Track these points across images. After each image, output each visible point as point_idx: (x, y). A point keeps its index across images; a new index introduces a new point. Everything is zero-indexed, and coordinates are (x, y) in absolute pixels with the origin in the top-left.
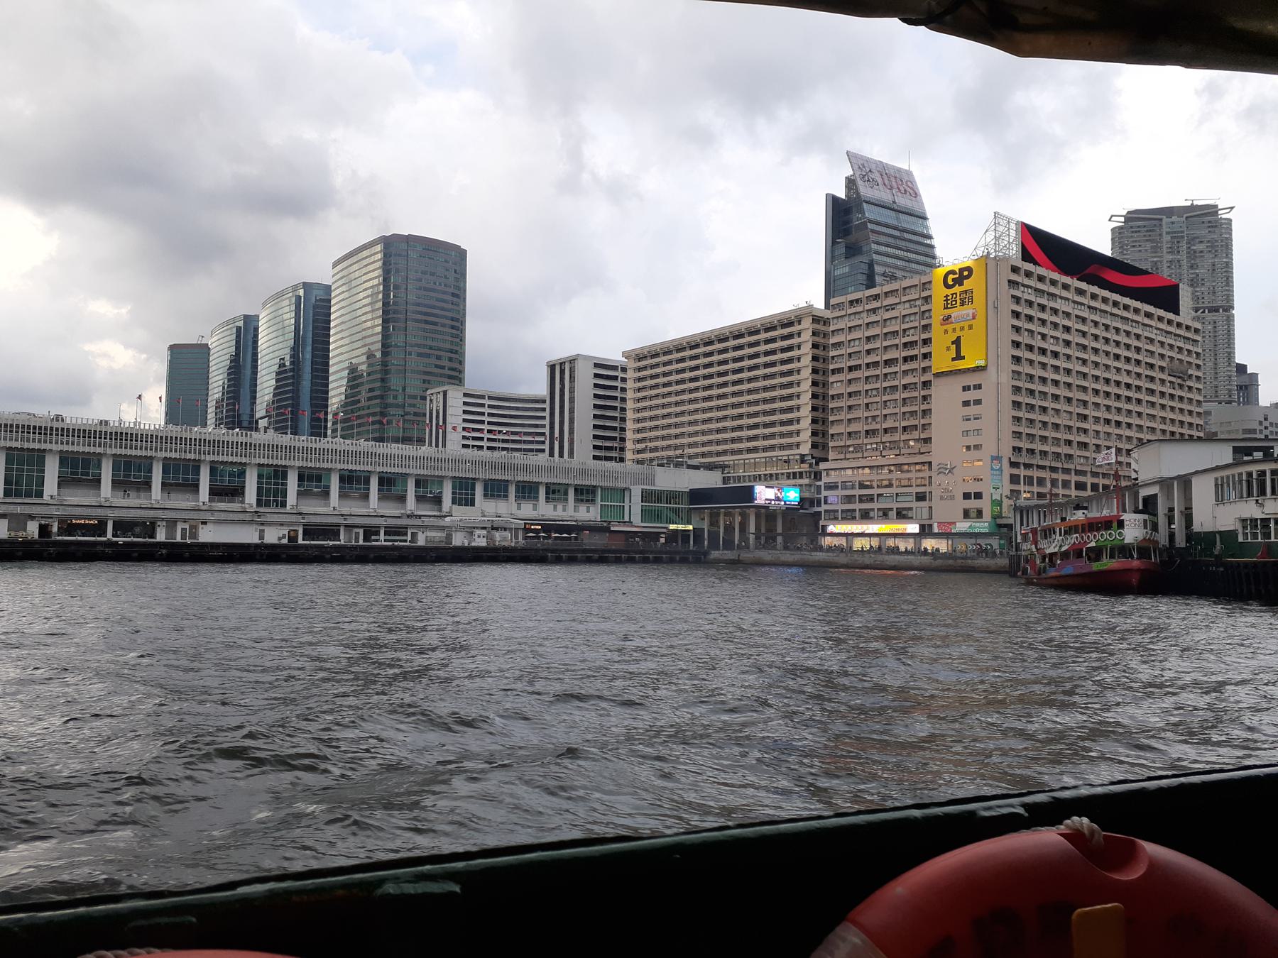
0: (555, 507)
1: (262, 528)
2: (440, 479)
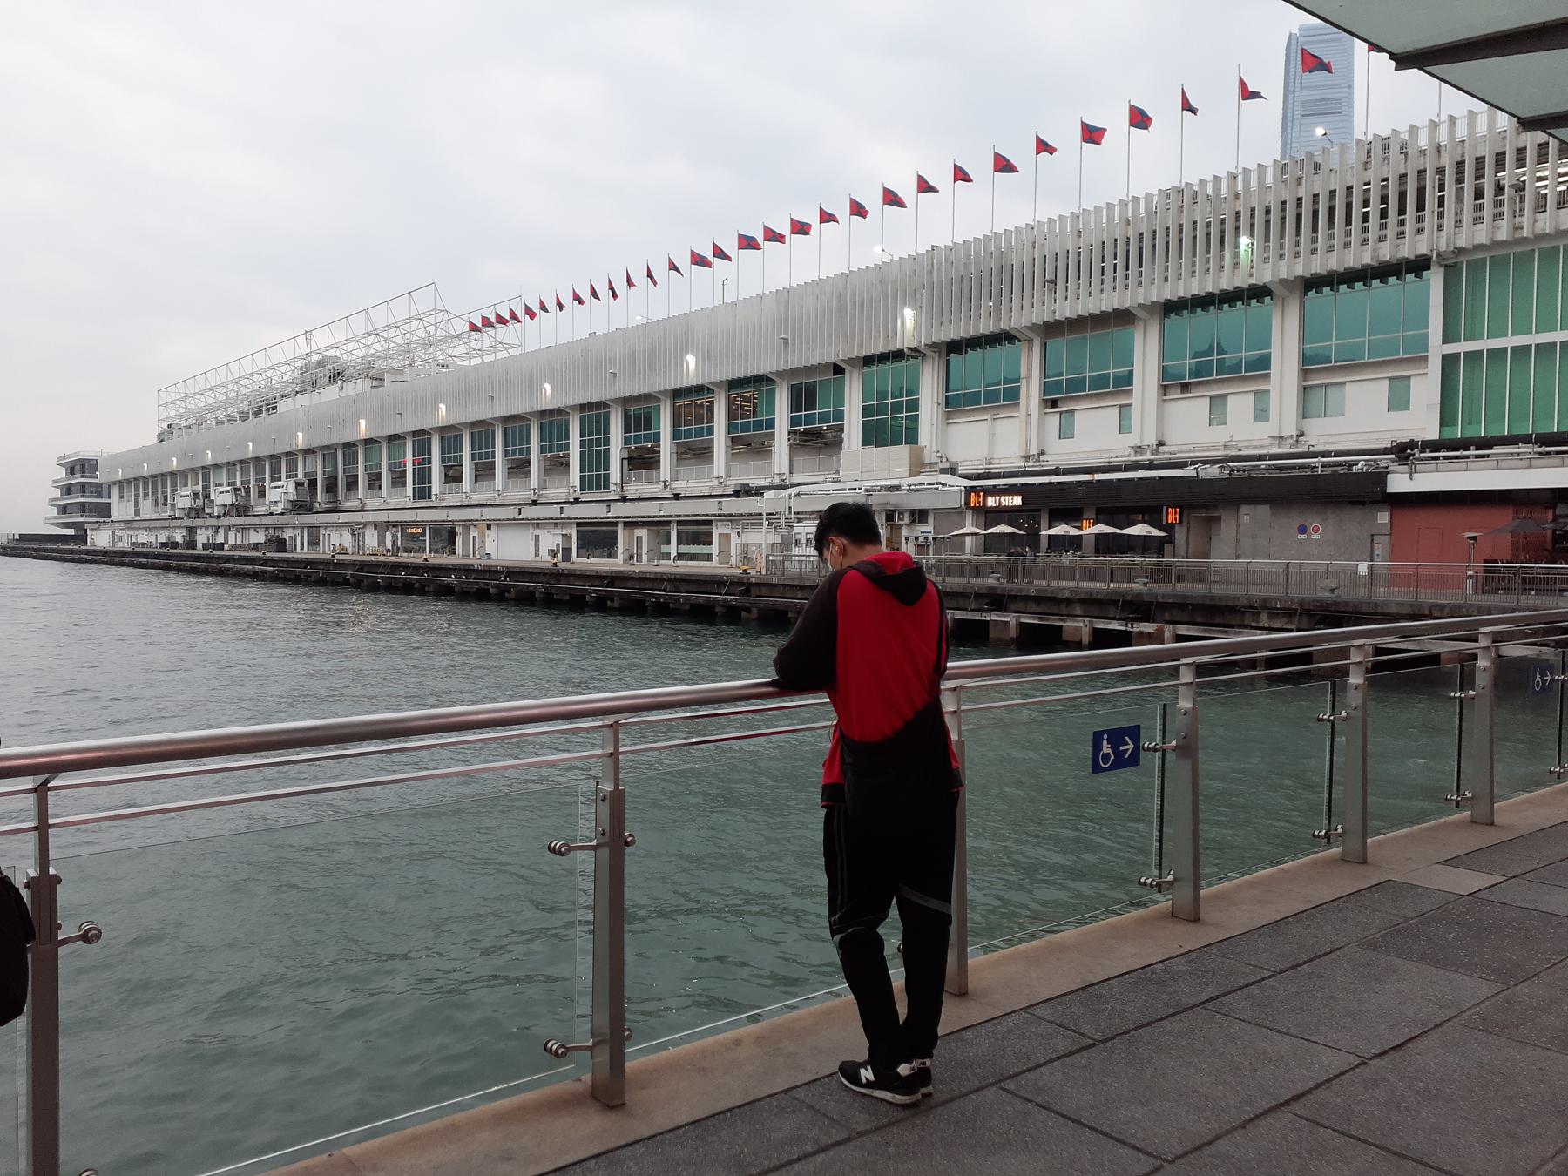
0: (1217, 402)
1: (537, 532)
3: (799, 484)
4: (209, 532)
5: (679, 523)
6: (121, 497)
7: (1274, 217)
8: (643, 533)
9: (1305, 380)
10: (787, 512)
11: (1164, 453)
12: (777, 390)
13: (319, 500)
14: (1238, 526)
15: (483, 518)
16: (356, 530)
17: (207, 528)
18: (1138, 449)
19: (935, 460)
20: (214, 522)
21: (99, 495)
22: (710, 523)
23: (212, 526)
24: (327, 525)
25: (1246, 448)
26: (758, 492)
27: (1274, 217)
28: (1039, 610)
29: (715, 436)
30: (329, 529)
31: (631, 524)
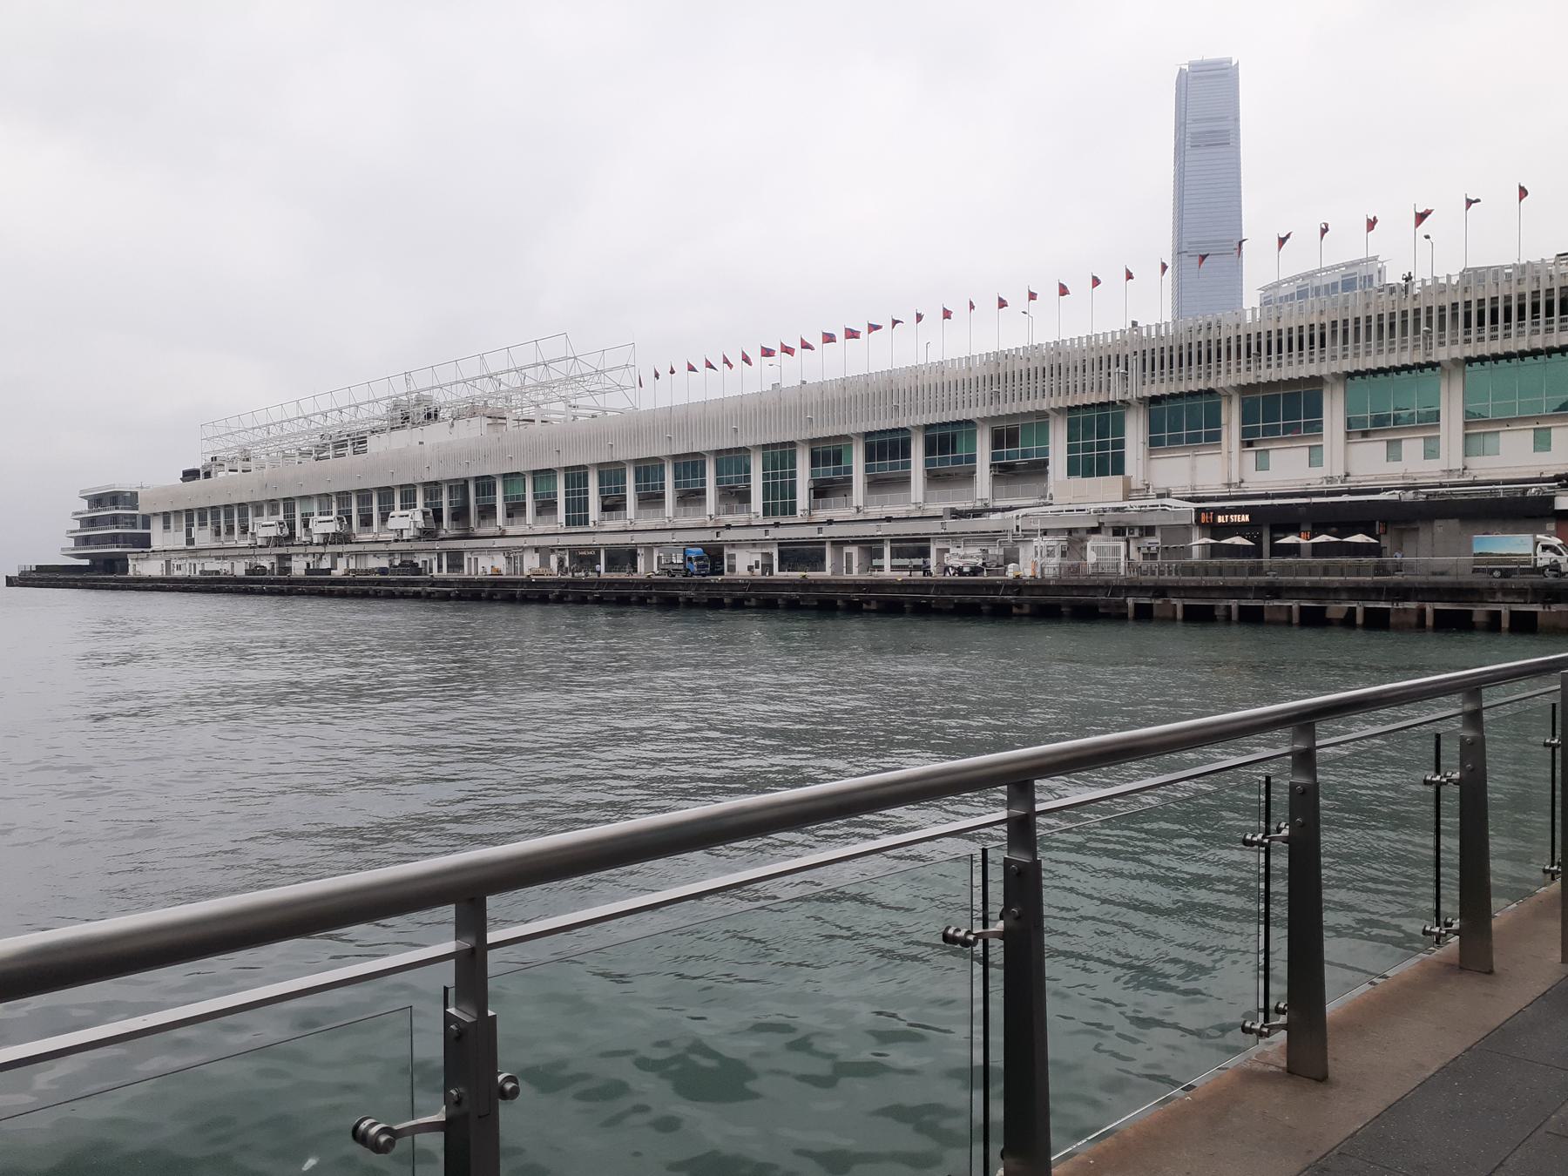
2: (1041, 419)
3: (1011, 509)
4: (310, 559)
5: (892, 541)
6: (166, 527)
7: (1448, 313)
8: (854, 550)
9: (1467, 429)
10: (1015, 530)
11: (1351, 482)
12: (978, 432)
13: (445, 526)
14: (1433, 534)
15: (674, 541)
16: (511, 555)
17: (306, 555)
18: (1330, 479)
19: (1140, 486)
20: (321, 549)
21: (134, 526)
22: (928, 540)
23: (314, 554)
24: (472, 550)
25: (1420, 478)
26: (977, 513)
27: (1448, 313)
28: (1310, 597)
29: (913, 469)
30: (476, 553)
31: (839, 543)
